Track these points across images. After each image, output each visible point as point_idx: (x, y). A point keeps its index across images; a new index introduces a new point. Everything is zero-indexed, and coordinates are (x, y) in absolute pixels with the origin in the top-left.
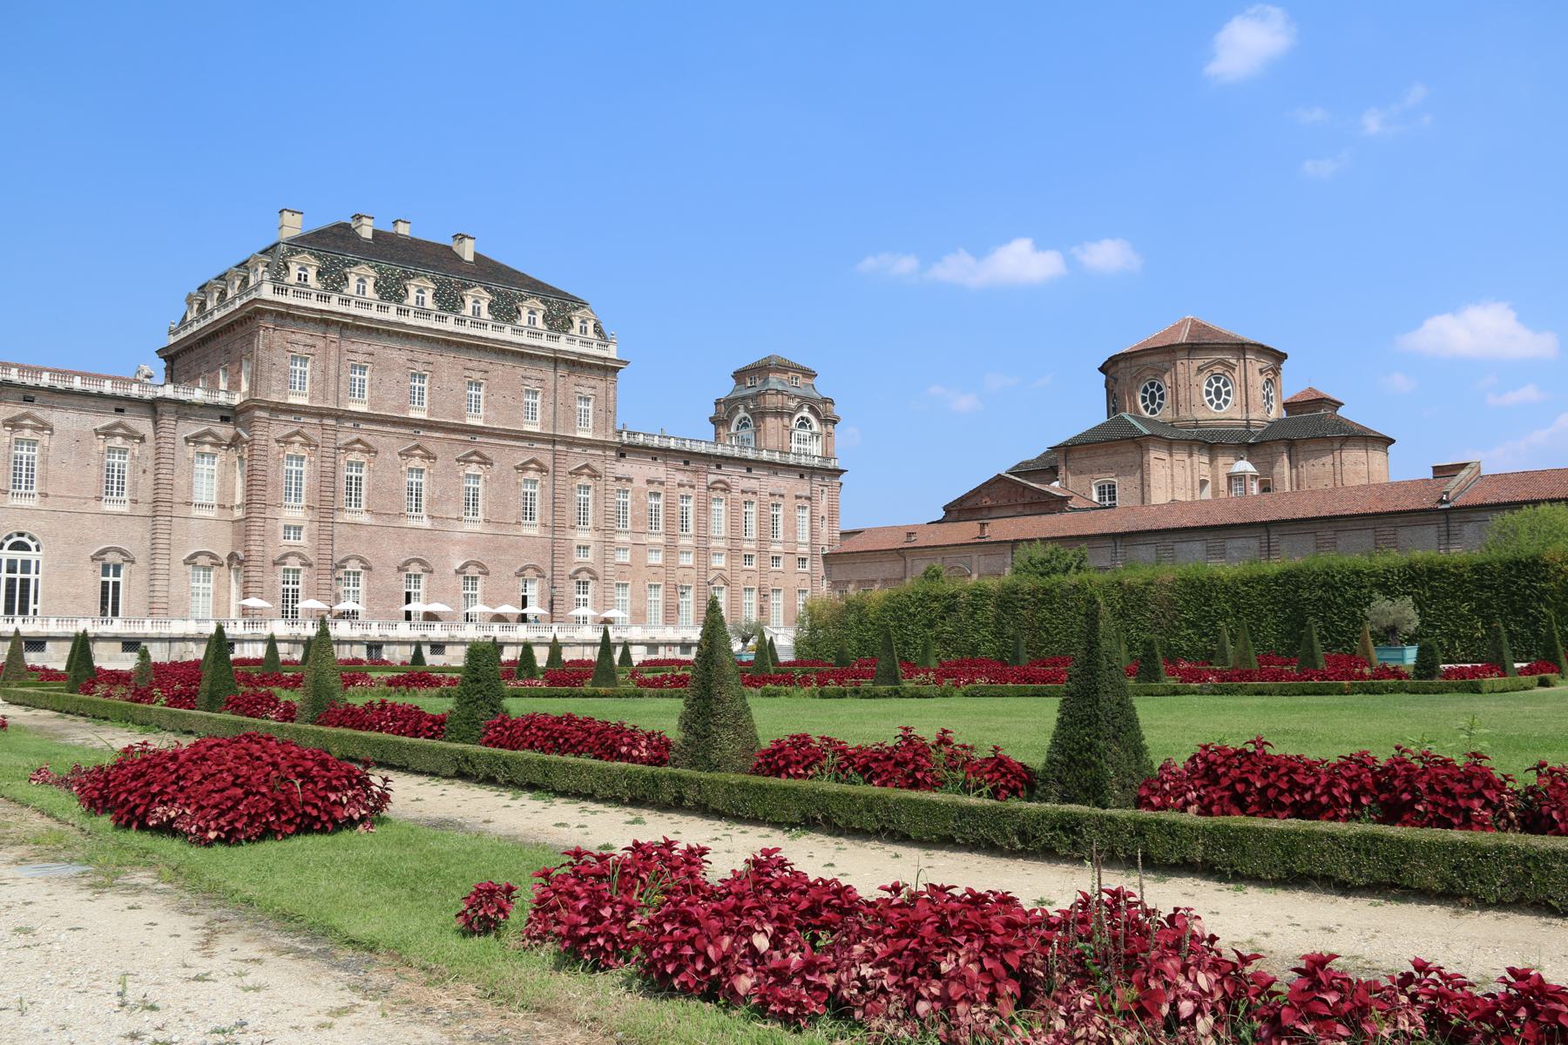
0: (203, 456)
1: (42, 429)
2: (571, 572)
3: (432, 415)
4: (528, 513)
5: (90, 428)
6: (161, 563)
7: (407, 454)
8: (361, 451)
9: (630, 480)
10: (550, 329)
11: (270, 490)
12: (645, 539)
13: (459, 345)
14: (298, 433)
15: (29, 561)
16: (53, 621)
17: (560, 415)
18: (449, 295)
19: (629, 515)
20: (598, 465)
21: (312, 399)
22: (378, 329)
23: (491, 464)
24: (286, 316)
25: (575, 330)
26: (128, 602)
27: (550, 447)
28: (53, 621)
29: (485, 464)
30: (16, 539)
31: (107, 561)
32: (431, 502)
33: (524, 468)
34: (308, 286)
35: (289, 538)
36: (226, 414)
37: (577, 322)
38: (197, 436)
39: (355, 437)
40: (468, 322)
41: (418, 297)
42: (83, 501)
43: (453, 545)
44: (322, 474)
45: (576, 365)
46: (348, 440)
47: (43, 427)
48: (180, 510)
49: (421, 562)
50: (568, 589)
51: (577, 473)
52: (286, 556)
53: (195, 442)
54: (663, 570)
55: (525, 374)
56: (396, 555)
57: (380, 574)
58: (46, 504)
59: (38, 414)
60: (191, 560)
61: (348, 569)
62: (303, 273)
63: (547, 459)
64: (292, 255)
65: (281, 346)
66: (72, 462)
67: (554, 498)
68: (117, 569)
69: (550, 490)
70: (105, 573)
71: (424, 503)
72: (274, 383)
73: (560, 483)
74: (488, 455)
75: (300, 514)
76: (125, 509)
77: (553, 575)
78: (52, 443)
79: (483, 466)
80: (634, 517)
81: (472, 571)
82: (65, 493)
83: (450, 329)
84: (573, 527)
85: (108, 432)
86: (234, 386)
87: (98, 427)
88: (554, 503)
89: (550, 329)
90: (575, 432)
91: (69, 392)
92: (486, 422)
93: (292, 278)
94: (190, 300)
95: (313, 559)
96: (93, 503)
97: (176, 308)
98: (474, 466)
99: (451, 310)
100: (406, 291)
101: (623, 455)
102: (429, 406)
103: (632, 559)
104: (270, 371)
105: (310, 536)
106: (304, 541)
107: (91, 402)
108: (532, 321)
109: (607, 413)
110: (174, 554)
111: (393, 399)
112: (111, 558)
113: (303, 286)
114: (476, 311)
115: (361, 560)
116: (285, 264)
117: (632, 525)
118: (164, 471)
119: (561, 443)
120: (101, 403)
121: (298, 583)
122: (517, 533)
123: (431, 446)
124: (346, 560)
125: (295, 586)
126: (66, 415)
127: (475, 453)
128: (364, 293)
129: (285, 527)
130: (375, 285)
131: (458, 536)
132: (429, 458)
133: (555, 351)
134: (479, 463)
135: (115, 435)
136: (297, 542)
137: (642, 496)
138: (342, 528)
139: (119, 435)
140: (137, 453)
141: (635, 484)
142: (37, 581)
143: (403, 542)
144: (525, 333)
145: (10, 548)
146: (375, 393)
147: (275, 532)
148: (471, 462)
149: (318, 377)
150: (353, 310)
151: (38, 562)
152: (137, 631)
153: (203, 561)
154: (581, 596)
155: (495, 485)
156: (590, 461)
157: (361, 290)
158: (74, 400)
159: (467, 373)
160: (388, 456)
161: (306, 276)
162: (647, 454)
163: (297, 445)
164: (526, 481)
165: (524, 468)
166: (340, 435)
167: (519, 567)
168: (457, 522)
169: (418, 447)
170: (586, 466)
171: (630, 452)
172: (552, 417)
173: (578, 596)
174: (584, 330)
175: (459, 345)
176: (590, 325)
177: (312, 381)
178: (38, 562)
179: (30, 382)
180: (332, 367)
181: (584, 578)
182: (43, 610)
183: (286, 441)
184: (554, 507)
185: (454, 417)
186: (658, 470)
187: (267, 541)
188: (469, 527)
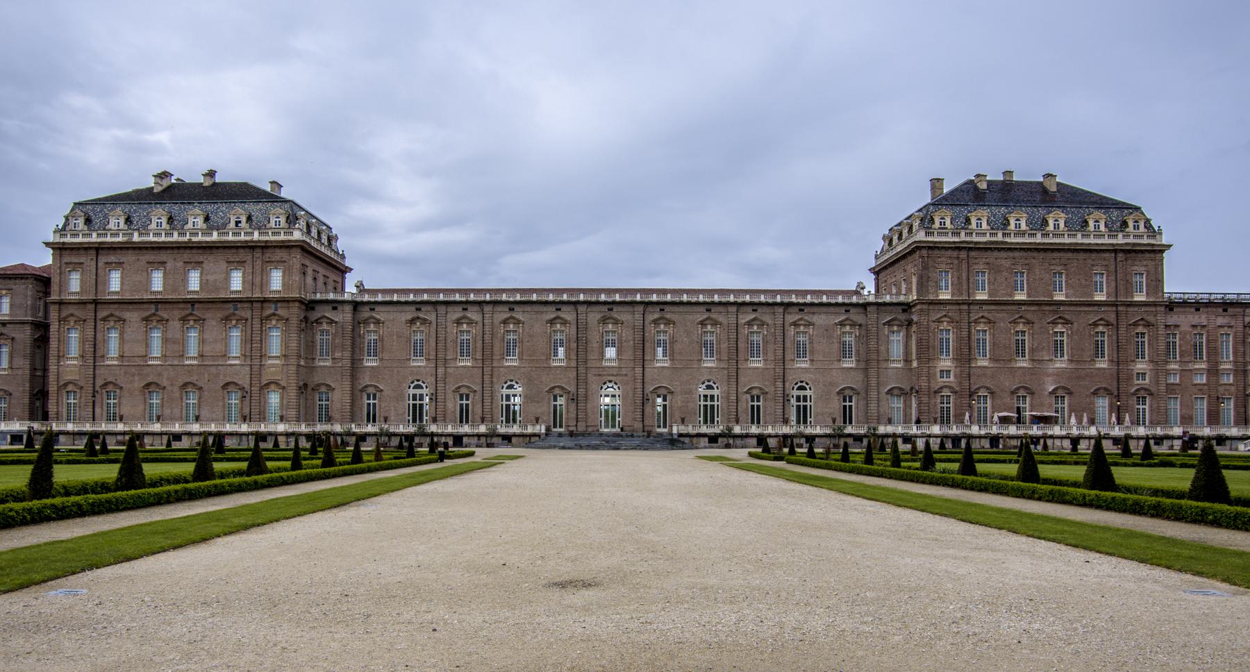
0: (893, 333)
1: (809, 325)
2: (1133, 390)
3: (1030, 297)
4: (1098, 351)
5: (832, 322)
6: (873, 394)
7: (1015, 322)
8: (985, 323)
9: (1177, 326)
10: (1110, 231)
11: (931, 350)
12: (1191, 366)
13: (1045, 250)
14: (945, 316)
15: (807, 396)
16: (818, 427)
17: (1121, 287)
18: (1037, 219)
19: (1178, 350)
20: (1151, 319)
21: (952, 295)
22: (991, 248)
23: (1072, 324)
24: (933, 247)
25: (1131, 228)
26: (857, 416)
27: (1114, 309)
28: (818, 427)
29: (1067, 324)
30: (799, 384)
31: (845, 394)
32: (1032, 350)
33: (1095, 324)
34: (946, 228)
35: (943, 377)
36: (906, 307)
37: (1131, 224)
38: (888, 322)
39: (980, 315)
40: (1051, 235)
41: (1016, 224)
42: (831, 362)
43: (1048, 376)
44: (959, 339)
45: (1132, 252)
46: (976, 317)
47: (809, 324)
48: (883, 365)
49: (1026, 388)
50: (1130, 402)
51: (1136, 324)
52: (942, 388)
53: (889, 325)
54: (1206, 387)
55: (1093, 263)
56: (1009, 383)
57: (1000, 396)
58: (813, 365)
59: (806, 318)
60: (890, 392)
61: (980, 394)
62: (943, 221)
63: (1112, 318)
64: (936, 211)
65: (932, 266)
66: (825, 341)
67: (1118, 343)
68: (851, 398)
69: (1115, 338)
70: (845, 401)
71: (1027, 351)
72: (930, 288)
73: (1122, 332)
74: (1070, 319)
75: (948, 363)
76: (853, 365)
77: (1119, 393)
78: (815, 333)
79: (1066, 326)
80: (1181, 351)
81: (1060, 393)
82: (822, 359)
83: (1038, 241)
84: (1133, 361)
85: (842, 324)
86: (909, 290)
87: (836, 321)
88: (1118, 346)
89: (1110, 231)
90: (1132, 297)
91: (821, 304)
92: (1067, 297)
93: (937, 225)
94: (884, 238)
95: (957, 389)
96: (836, 363)
97: (880, 244)
98: (1060, 326)
99: (1039, 229)
100: (1008, 221)
101: (1171, 310)
102: (1027, 291)
103: (1180, 381)
104: (928, 281)
105: (955, 376)
106: (952, 378)
107: (832, 309)
108: (1097, 227)
109: (1156, 282)
110: (881, 388)
111: (1003, 290)
112: (847, 392)
113: (943, 228)
114: (1056, 226)
115: (988, 388)
116: (932, 217)
117: (1180, 357)
118: (873, 343)
119: (1121, 305)
120: (837, 309)
121: (949, 403)
122: (1092, 367)
123: (1029, 316)
124: (979, 388)
125: (948, 405)
126: (820, 316)
127: (1060, 318)
128: (981, 227)
129: (941, 371)
130: (988, 221)
131: (1050, 371)
132: (1029, 323)
133: (1112, 244)
134: (1063, 323)
135: (845, 325)
136: (948, 380)
137: (1188, 337)
138: (974, 370)
139: (848, 325)
140: (858, 334)
141: (1182, 329)
142: (811, 406)
143: (1014, 377)
144: (1092, 236)
145: (797, 389)
146: (992, 287)
147: (935, 374)
148: (1058, 323)
149: (956, 282)
150: (975, 239)
151: (811, 396)
152: (860, 432)
153: (896, 392)
154: (1141, 407)
155: (1076, 337)
156: (1145, 316)
157: (979, 225)
158: (824, 309)
159: (1052, 267)
160: (1002, 324)
161: (944, 222)
162: (1191, 307)
163: (945, 323)
164: (1097, 333)
165: (1095, 324)
166: (971, 315)
167: (1094, 389)
168: (1050, 363)
169: (1021, 317)
170: (1142, 319)
171: (1177, 306)
172: (1114, 289)
173: (1138, 407)
174: (1136, 227)
175: (1045, 250)
176: (1142, 225)
177: (952, 285)
178: (811, 396)
179: (801, 301)
180: (964, 275)
181: (1142, 394)
182: (814, 421)
183: (939, 321)
184: (1118, 348)
185: (1045, 297)
186: (1201, 318)
187: (931, 379)
188: (1058, 365)
